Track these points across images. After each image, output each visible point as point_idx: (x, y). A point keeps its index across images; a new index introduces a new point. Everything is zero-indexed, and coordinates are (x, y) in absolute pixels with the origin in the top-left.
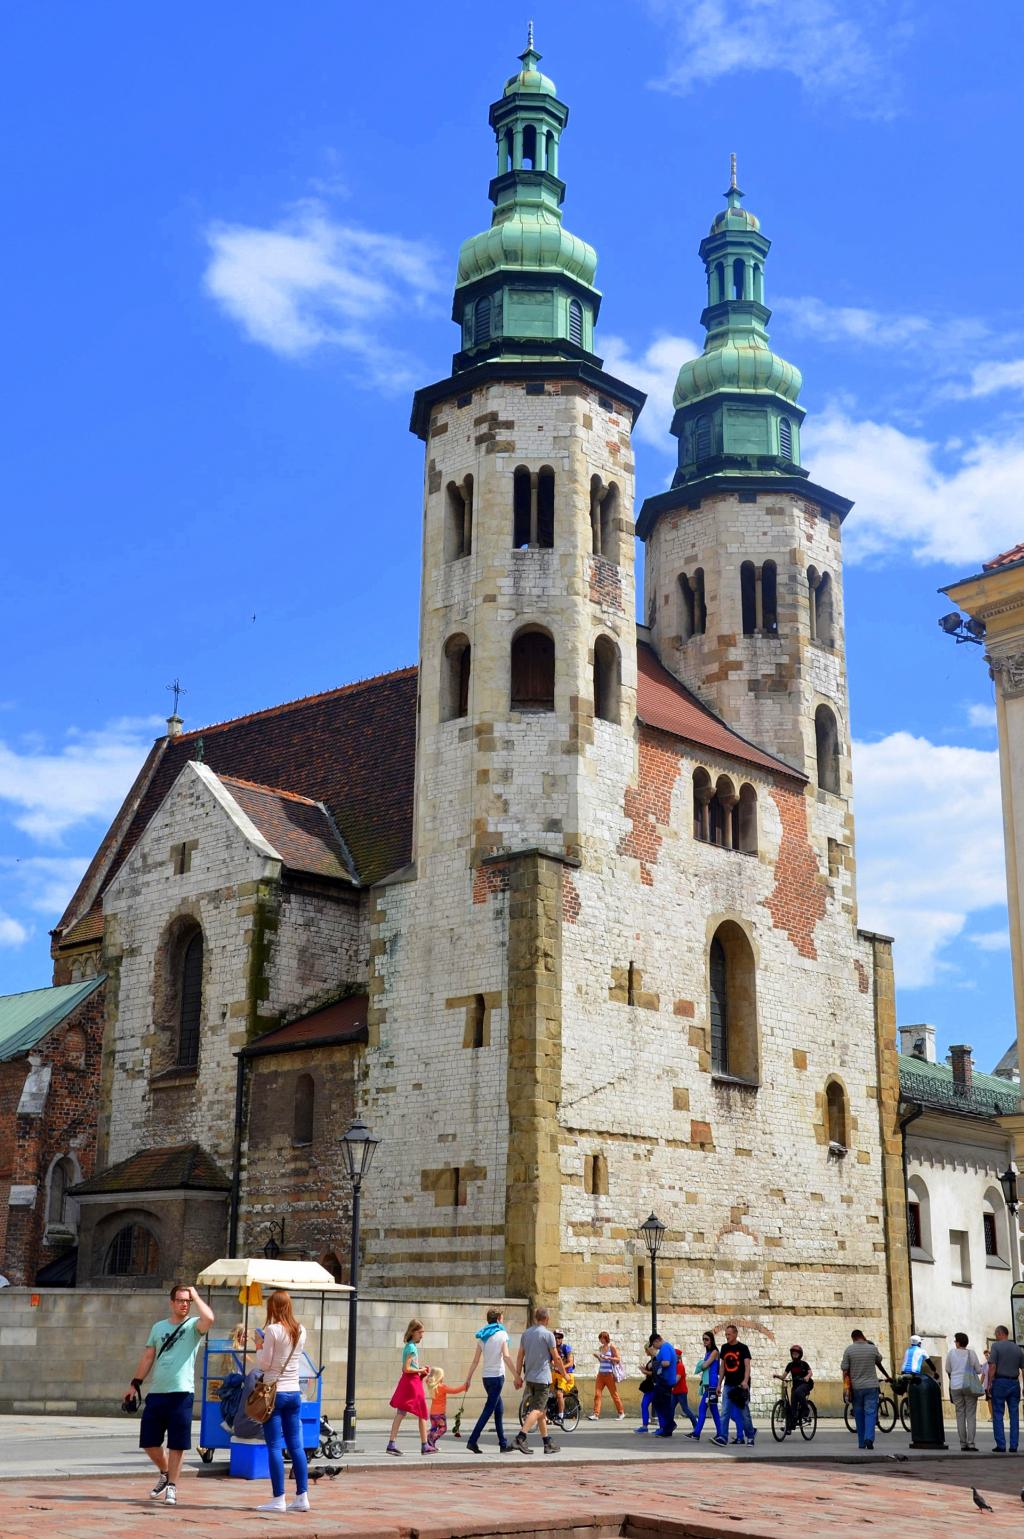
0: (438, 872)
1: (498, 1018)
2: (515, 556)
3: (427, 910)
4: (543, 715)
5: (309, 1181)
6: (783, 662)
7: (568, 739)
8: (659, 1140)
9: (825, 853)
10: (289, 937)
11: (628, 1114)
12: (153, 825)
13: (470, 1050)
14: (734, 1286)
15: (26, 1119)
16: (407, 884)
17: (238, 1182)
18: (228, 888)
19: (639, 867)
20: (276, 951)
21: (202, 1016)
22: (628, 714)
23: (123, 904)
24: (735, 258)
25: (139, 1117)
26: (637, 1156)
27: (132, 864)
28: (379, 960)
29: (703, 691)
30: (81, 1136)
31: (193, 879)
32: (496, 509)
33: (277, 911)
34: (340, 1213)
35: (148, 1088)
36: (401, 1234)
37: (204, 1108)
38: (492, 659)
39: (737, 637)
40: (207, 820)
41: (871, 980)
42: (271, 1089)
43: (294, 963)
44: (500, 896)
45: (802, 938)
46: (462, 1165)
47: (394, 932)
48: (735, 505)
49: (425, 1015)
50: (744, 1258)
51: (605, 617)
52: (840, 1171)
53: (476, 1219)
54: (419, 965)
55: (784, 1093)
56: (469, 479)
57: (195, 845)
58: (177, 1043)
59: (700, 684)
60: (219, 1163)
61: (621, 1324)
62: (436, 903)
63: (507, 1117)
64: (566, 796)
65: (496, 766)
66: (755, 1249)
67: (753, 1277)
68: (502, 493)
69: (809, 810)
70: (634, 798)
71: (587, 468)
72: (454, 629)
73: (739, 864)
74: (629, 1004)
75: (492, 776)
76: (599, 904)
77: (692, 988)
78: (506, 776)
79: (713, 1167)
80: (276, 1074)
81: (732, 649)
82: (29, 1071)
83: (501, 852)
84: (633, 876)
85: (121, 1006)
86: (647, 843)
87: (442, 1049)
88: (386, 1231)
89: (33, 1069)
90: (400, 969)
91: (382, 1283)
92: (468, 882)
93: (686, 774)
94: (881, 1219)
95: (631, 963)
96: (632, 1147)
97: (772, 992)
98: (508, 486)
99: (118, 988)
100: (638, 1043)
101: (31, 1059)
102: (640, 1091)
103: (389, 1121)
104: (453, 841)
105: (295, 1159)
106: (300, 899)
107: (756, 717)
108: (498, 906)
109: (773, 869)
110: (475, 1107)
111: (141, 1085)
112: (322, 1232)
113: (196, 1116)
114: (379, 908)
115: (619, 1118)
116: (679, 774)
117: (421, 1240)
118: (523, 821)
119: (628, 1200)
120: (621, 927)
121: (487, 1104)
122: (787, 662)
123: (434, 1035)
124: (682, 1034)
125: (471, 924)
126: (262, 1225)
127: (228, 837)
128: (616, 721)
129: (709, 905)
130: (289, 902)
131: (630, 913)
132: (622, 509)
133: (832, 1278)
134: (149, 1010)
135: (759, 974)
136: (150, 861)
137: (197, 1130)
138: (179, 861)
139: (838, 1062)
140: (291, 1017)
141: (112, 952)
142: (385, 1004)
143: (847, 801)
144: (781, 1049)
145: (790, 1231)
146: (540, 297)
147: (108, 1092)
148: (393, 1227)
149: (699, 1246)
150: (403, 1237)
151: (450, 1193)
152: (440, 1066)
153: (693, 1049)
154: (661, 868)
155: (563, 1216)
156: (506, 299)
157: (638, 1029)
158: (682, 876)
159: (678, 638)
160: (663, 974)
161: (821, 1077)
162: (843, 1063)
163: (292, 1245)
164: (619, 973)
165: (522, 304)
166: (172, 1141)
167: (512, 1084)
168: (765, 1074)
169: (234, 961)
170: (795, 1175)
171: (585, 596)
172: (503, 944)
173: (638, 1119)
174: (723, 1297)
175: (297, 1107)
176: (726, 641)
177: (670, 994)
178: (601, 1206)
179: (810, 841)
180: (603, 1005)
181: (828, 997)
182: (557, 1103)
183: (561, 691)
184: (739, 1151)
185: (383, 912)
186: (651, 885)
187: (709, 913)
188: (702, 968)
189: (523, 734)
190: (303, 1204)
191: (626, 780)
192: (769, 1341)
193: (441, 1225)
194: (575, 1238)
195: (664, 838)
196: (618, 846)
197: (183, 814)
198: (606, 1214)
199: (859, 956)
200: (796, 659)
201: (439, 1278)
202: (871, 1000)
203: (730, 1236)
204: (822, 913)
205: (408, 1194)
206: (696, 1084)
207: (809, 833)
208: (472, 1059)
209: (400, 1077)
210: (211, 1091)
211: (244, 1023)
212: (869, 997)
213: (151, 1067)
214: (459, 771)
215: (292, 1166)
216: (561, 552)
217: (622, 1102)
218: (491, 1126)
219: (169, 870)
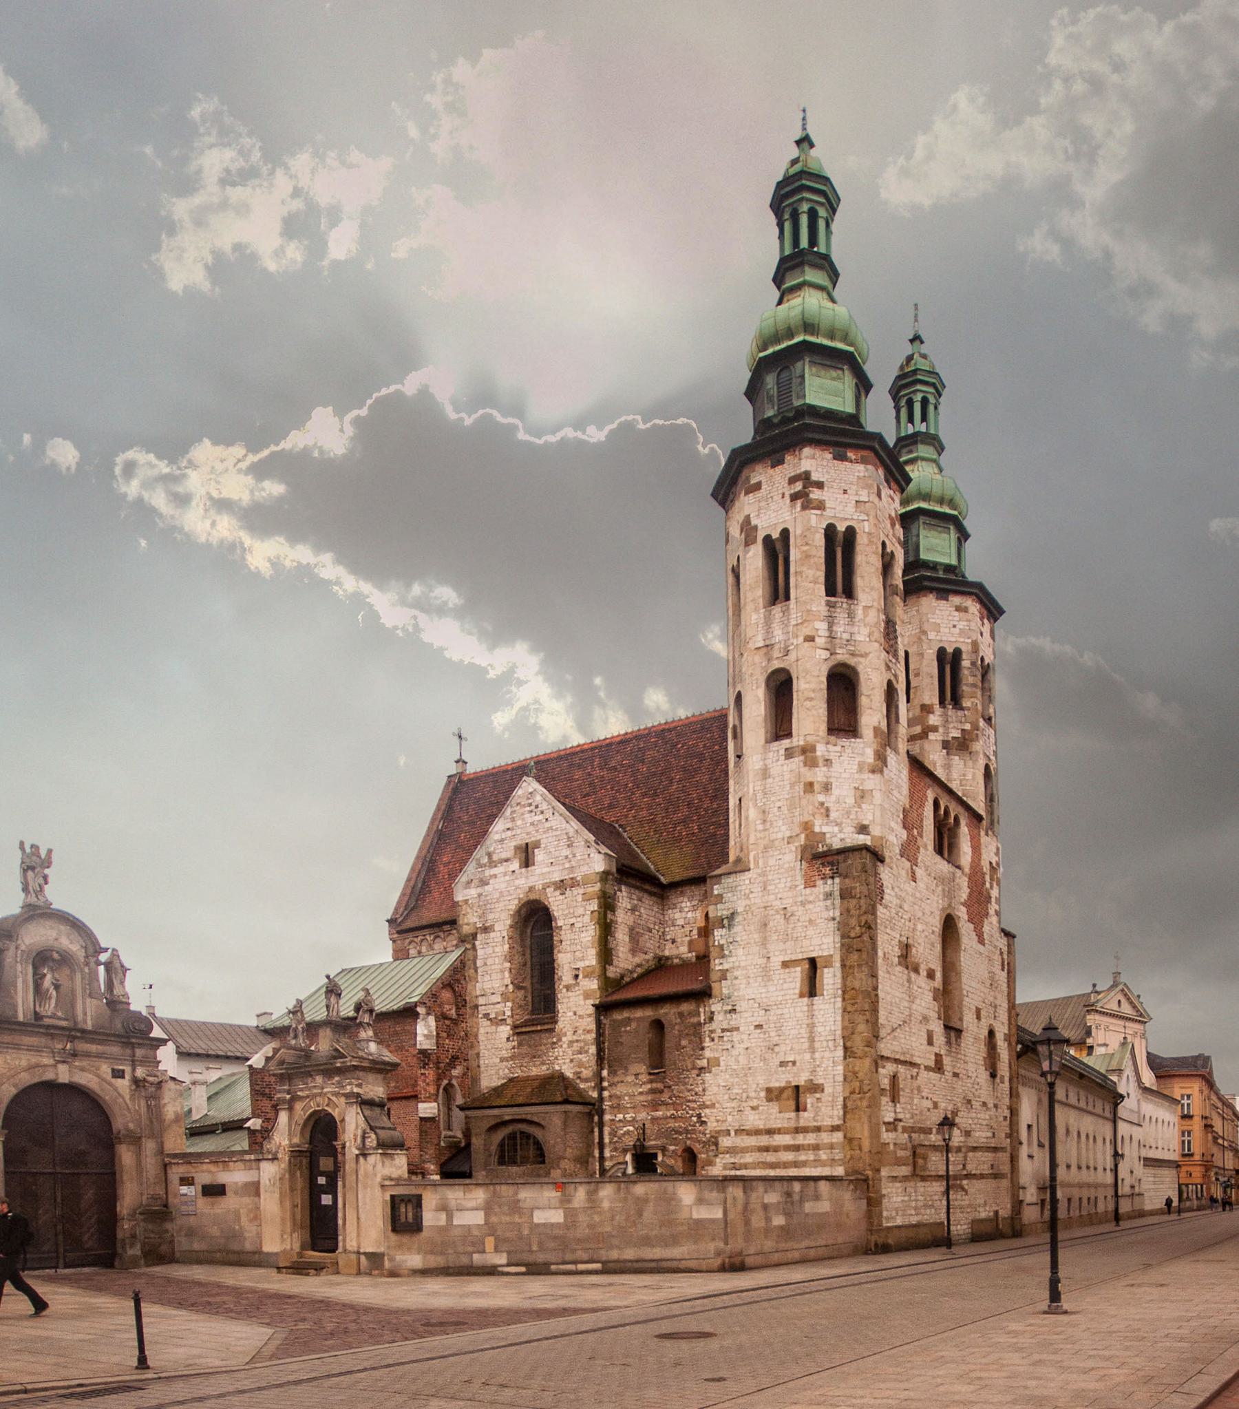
0: (770, 864)
1: (830, 975)
3: (760, 894)
5: (665, 1097)
10: (623, 918)
12: (495, 829)
13: (806, 1000)
15: (423, 1052)
17: (601, 1099)
18: (572, 879)
21: (556, 977)
23: (473, 892)
25: (505, 1054)
27: (478, 860)
28: (718, 933)
30: (458, 1067)
31: (538, 872)
33: (614, 897)
34: (695, 1119)
36: (749, 1133)
37: (565, 1046)
40: (547, 825)
42: (626, 1031)
43: (627, 939)
44: (830, 882)
47: (731, 911)
53: (815, 1121)
57: (537, 845)
58: (529, 998)
60: (582, 1086)
62: (769, 888)
78: (827, 788)
80: (628, 1021)
82: (418, 1018)
83: (825, 848)
85: (479, 971)
87: (780, 998)
88: (736, 1132)
89: (421, 1017)
90: (738, 939)
92: (798, 871)
99: (475, 957)
101: (418, 1009)
103: (734, 1052)
104: (783, 839)
105: (651, 1082)
108: (828, 889)
110: (812, 1040)
111: (505, 1030)
112: (681, 1133)
113: (558, 1052)
114: (716, 892)
117: (767, 1136)
118: (841, 823)
121: (822, 1039)
123: (772, 988)
125: (803, 904)
126: (625, 1129)
127: (569, 838)
134: (507, 974)
136: (495, 857)
138: (523, 859)
140: (627, 979)
141: (466, 930)
142: (726, 966)
147: (476, 1036)
151: (792, 1103)
152: (779, 1012)
163: (653, 1143)
167: (847, 1023)
169: (583, 935)
172: (834, 919)
175: (649, 1044)
185: (720, 896)
193: (785, 1125)
197: (523, 819)
205: (755, 1103)
208: (808, 1005)
209: (743, 1021)
211: (596, 981)
215: (649, 1086)
218: (827, 1054)
219: (515, 865)
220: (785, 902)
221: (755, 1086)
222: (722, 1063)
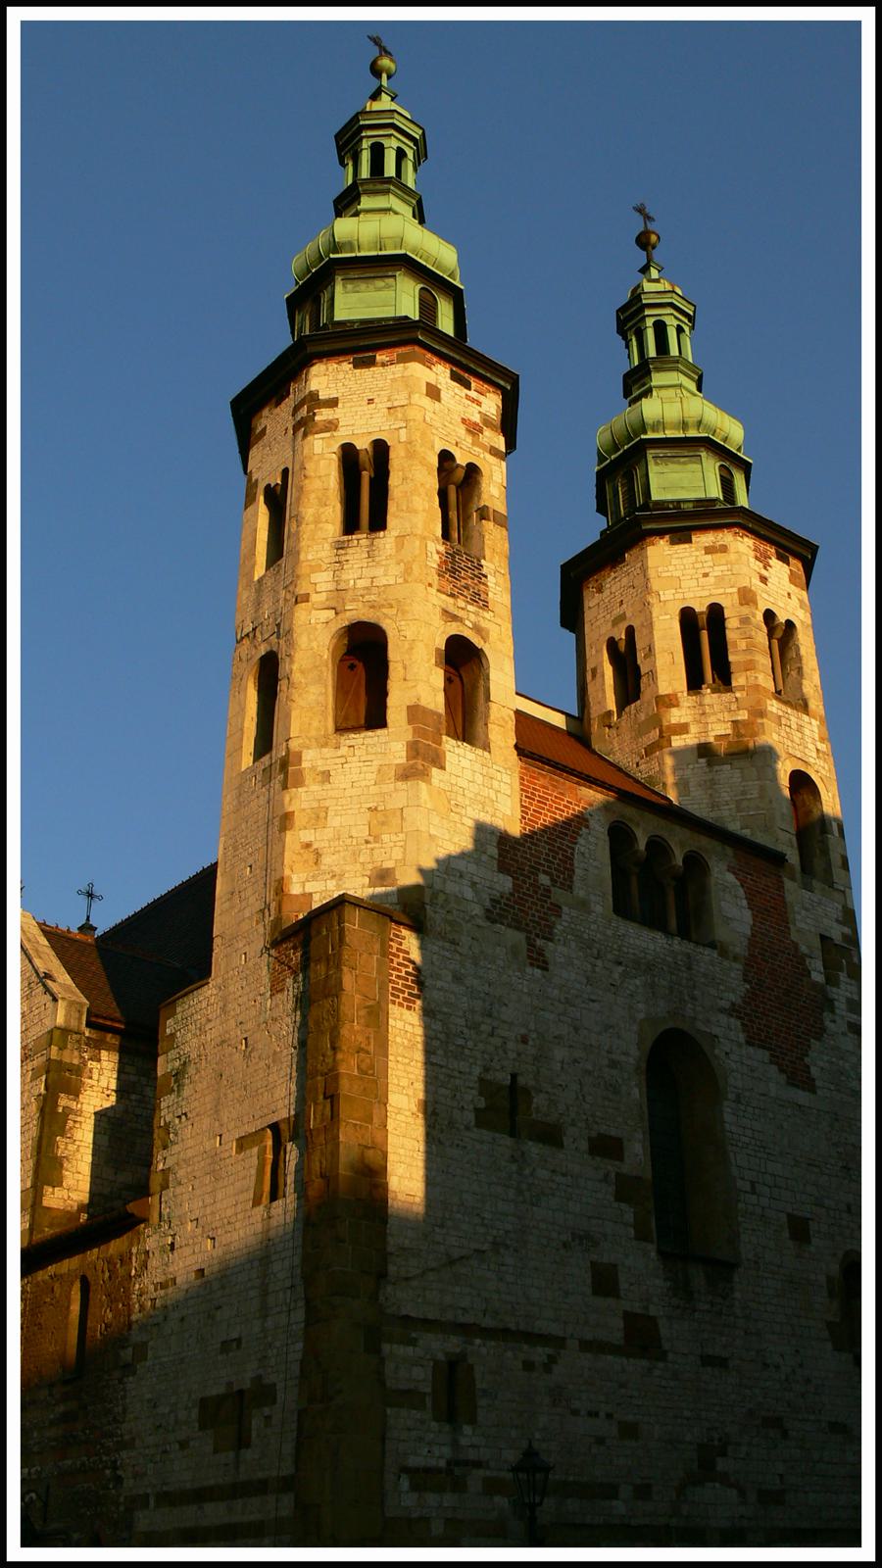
6: (739, 718)
7: (404, 760)
16: (199, 991)
19: (524, 941)
20: (75, 1122)
22: (501, 734)
26: (528, 1366)
29: (642, 767)
32: (313, 496)
33: (78, 1070)
39: (679, 695)
45: (791, 1062)
46: (247, 1385)
48: (666, 548)
51: (461, 613)
59: (638, 759)
63: (301, 1303)
64: (402, 836)
68: (320, 477)
69: (789, 898)
70: (514, 848)
72: (263, 650)
73: (688, 956)
74: (512, 1134)
77: (620, 1119)
78: (319, 817)
79: (664, 1383)
81: (674, 710)
86: (537, 911)
87: (229, 1212)
93: (597, 827)
95: (514, 1076)
97: (749, 1133)
107: (711, 788)
109: (741, 967)
114: (168, 1031)
116: (587, 827)
118: (342, 875)
119: (514, 1433)
122: (746, 718)
128: (486, 747)
129: (641, 1006)
130: (99, 1060)
132: (484, 496)
142: (170, 1162)
143: (844, 892)
146: (380, 283)
148: (165, 1488)
153: (623, 1206)
154: (560, 948)
156: (339, 288)
157: (527, 1172)
158: (599, 963)
161: (835, 1255)
165: (358, 292)
171: (430, 585)
176: (670, 701)
178: (464, 1441)
179: (794, 936)
182: (382, 1275)
184: (708, 1361)
185: (173, 1035)
186: (545, 969)
187: (641, 1016)
188: (635, 1093)
189: (343, 760)
190: (69, 1462)
194: (416, 1495)
195: (564, 907)
196: (488, 910)
198: (472, 1455)
204: (820, 1033)
207: (791, 926)
214: (260, 824)
217: (501, 1280)
220: (244, 1027)
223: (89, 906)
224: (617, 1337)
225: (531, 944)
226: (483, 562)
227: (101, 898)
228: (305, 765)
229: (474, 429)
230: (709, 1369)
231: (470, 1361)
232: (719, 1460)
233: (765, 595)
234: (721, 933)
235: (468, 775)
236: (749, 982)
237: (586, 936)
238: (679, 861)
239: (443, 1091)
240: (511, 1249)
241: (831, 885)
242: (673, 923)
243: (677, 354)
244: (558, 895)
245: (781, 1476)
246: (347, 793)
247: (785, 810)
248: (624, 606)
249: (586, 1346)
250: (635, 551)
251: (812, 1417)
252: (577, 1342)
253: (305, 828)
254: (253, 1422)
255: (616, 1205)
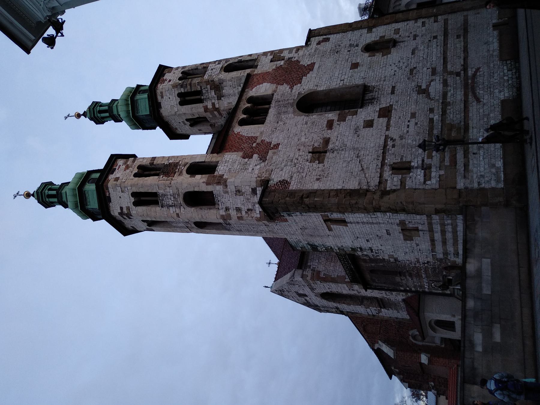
2: (162, 207)
4: (215, 196)
8: (387, 134)
9: (275, 63)
11: (374, 151)
14: (455, 90)
17: (416, 292)
24: (98, 114)
25: (395, 312)
26: (393, 146)
34: (426, 265)
35: (384, 309)
37: (389, 297)
38: (198, 215)
39: (204, 105)
41: (325, 37)
46: (400, 228)
47: (308, 245)
49: (338, 238)
50: (441, 85)
52: (403, 42)
54: (318, 238)
55: (368, 73)
56: (143, 221)
59: (223, 117)
61: (475, 151)
62: (292, 233)
64: (243, 186)
65: (235, 214)
66: (437, 81)
67: (450, 81)
68: (143, 211)
69: (260, 72)
70: (246, 154)
71: (131, 179)
72: (193, 225)
74: (326, 152)
75: (239, 215)
76: (284, 170)
77: (322, 121)
78: (238, 210)
79: (399, 105)
81: (208, 107)
84: (274, 153)
85: (356, 312)
87: (350, 233)
89: (380, 347)
91: (456, 254)
93: (240, 130)
94: (423, 20)
95: (309, 152)
96: (389, 149)
97: (326, 82)
98: (141, 209)
100: (343, 148)
101: (376, 348)
102: (364, 146)
105: (405, 276)
106: (309, 261)
111: (382, 310)
114: (300, 249)
115: (375, 156)
116: (240, 133)
117: (436, 242)
119: (414, 150)
120: (294, 158)
124: (341, 125)
128: (218, 162)
131: (289, 154)
132: (147, 163)
133: (450, 41)
134: (356, 306)
135: (319, 89)
137: (397, 299)
139: (356, 48)
142: (337, 248)
143: (258, 55)
144: (350, 76)
145: (429, 63)
146: (87, 195)
149: (436, 108)
150: (435, 247)
151: (413, 232)
152: (357, 234)
153: (347, 119)
154: (273, 139)
155: (421, 187)
156: (89, 207)
157: (337, 148)
158: (278, 128)
159: (211, 125)
160: (315, 136)
162: (357, 46)
163: (441, 279)
164: (313, 158)
166: (403, 305)
168: (360, 82)
169: (333, 286)
170: (404, 63)
172: (301, 213)
173: (376, 146)
174: (460, 95)
176: (206, 109)
177: (323, 132)
178: (416, 165)
179: (271, 70)
180: (326, 166)
181: (330, 55)
182: (367, 191)
183: (205, 188)
184: (393, 92)
185: (301, 248)
187: (293, 115)
188: (314, 117)
189: (222, 203)
190: (423, 275)
191: (239, 158)
192: (481, 70)
193: (428, 235)
196: (263, 161)
198: (420, 162)
199: (315, 43)
200: (207, 82)
201: (454, 236)
202: (332, 36)
203: (431, 94)
204: (298, 61)
206: (362, 116)
207: (268, 71)
210: (382, 295)
212: (332, 37)
213: (376, 308)
216: (158, 189)
217: (368, 155)
220: (298, 229)
221: (404, 245)
222: (392, 254)
223: (272, 263)
224: (386, 120)
225: (272, 148)
226: (165, 164)
227: (270, 261)
228: (224, 214)
229: (127, 167)
230: (395, 92)
231: (392, 163)
232: (422, 88)
233: (174, 81)
234: (269, 92)
235: (225, 167)
236: (283, 83)
237: (270, 132)
238: (249, 105)
239: (313, 174)
240: (359, 152)
241: (256, 59)
242: (267, 106)
243: (107, 107)
244: (258, 141)
245: (427, 69)
246: (231, 202)
247: (235, 74)
248: (180, 122)
249: (388, 129)
250: (164, 119)
251: (410, 60)
252: (387, 132)
253: (242, 213)
254: (410, 226)
255: (346, 121)
